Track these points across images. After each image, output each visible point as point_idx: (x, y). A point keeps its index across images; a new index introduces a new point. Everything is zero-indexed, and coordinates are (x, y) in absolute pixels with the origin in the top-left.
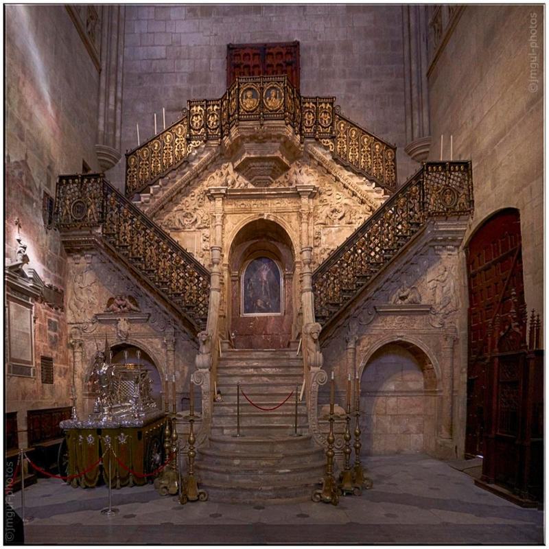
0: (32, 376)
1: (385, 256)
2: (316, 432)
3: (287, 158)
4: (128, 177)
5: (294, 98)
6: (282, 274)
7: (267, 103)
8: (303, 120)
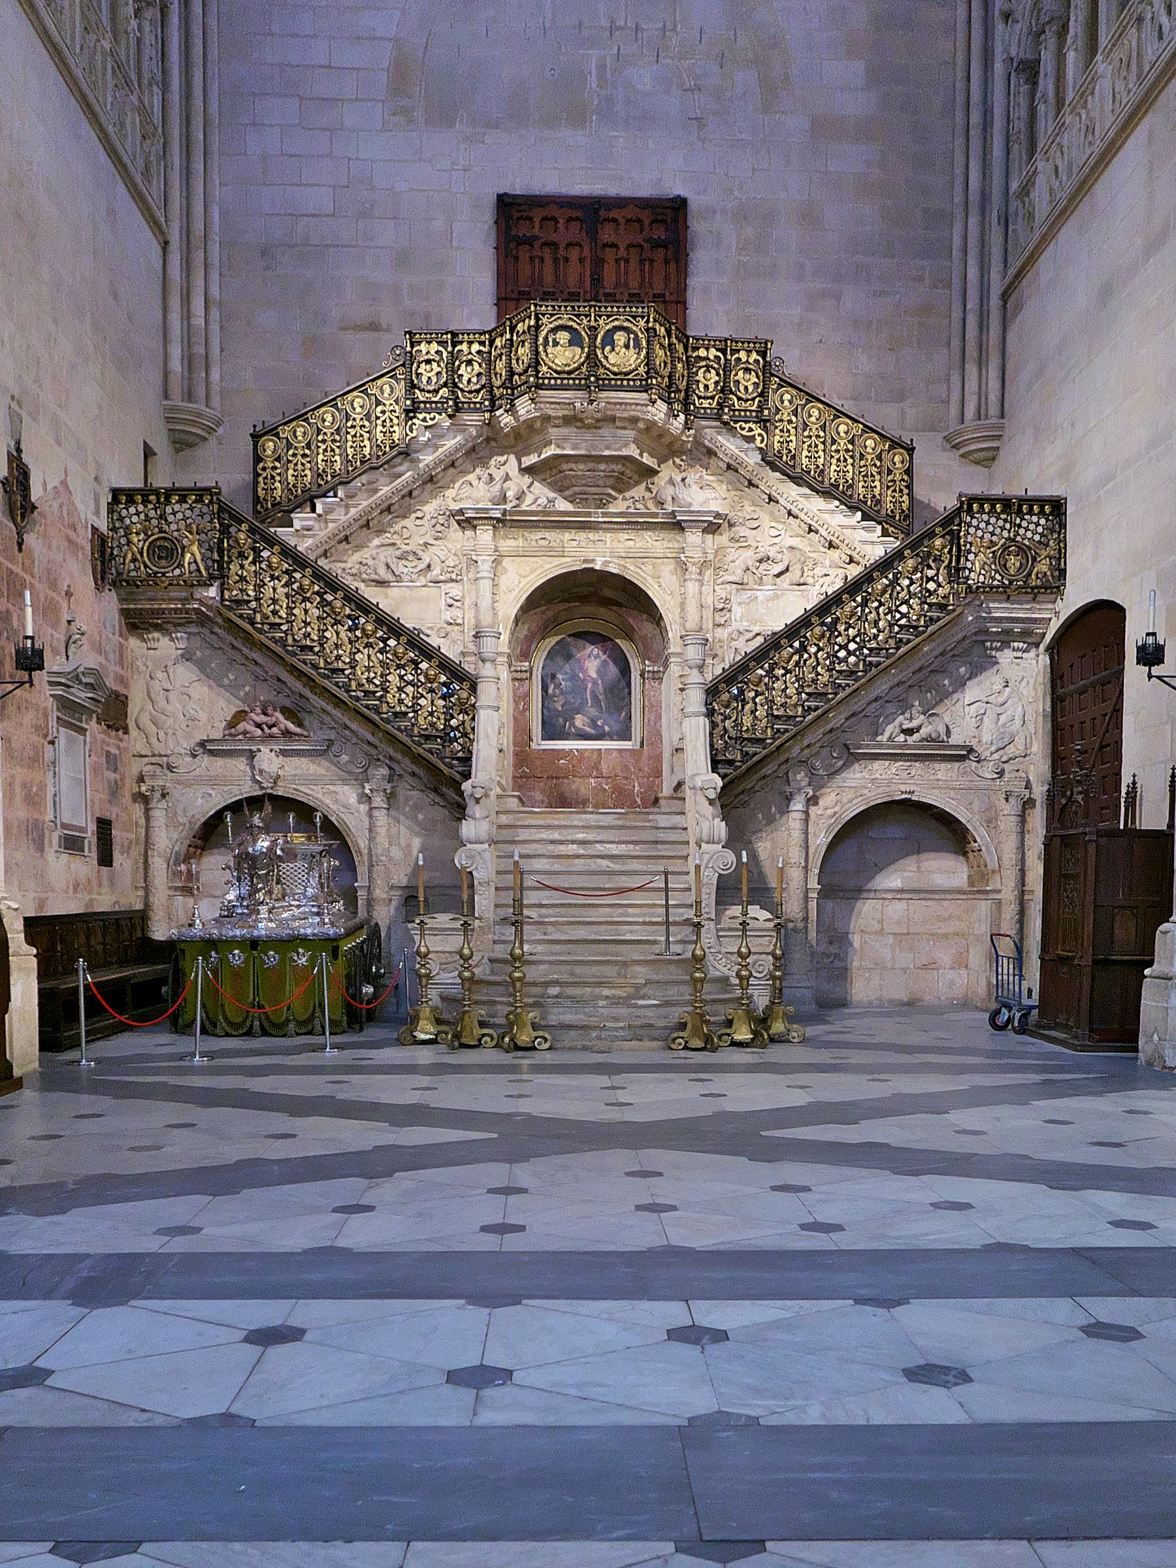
0: (86, 853)
2: (713, 950)
4: (261, 479)
6: (635, 665)
7: (606, 358)
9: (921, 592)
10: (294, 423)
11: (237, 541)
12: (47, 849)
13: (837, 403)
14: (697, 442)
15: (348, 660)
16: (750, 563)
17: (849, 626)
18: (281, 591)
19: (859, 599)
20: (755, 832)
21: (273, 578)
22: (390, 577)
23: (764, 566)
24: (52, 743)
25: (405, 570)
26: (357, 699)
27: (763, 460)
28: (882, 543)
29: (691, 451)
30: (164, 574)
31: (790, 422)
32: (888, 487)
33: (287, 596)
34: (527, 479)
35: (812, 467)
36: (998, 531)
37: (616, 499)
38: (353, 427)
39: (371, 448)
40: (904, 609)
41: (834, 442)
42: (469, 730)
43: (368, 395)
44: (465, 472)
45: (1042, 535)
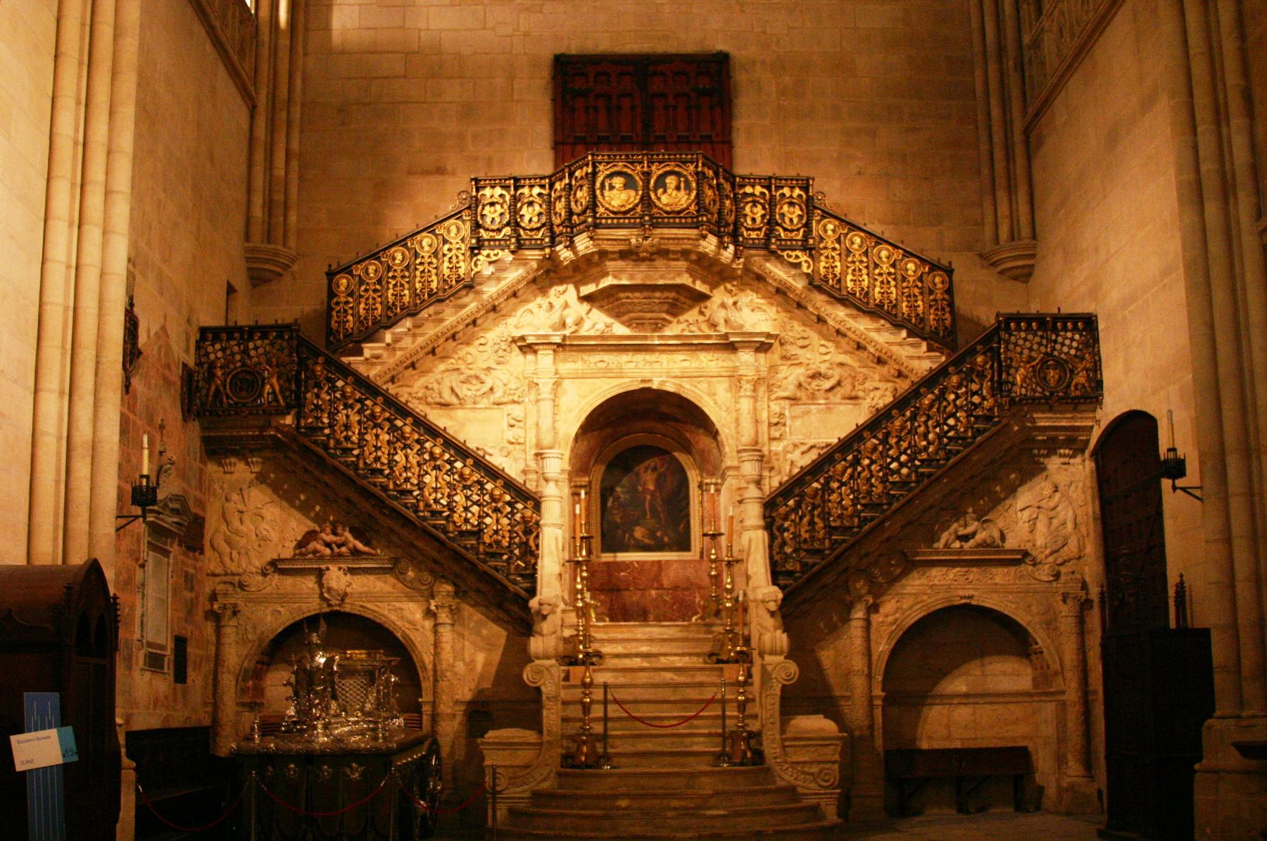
1: (921, 470)
2: (779, 760)
3: (704, 282)
4: (334, 313)
5: (718, 184)
8: (739, 213)
9: (966, 405)
10: (367, 262)
11: (313, 372)
12: (134, 666)
13: (876, 229)
14: (747, 269)
15: (415, 482)
16: (802, 379)
17: (900, 439)
18: (355, 418)
19: (908, 413)
20: (818, 641)
21: (346, 406)
22: (454, 400)
23: (815, 383)
24: (143, 566)
25: (469, 393)
26: (425, 519)
27: (810, 284)
28: (929, 358)
29: (740, 276)
30: (244, 405)
31: (834, 249)
32: (931, 306)
33: (359, 422)
34: (586, 306)
35: (858, 290)
36: (1035, 347)
37: (670, 322)
38: (421, 264)
39: (438, 282)
40: (951, 422)
41: (876, 266)
42: (534, 548)
43: (436, 235)
44: (526, 301)
45: (1077, 349)
